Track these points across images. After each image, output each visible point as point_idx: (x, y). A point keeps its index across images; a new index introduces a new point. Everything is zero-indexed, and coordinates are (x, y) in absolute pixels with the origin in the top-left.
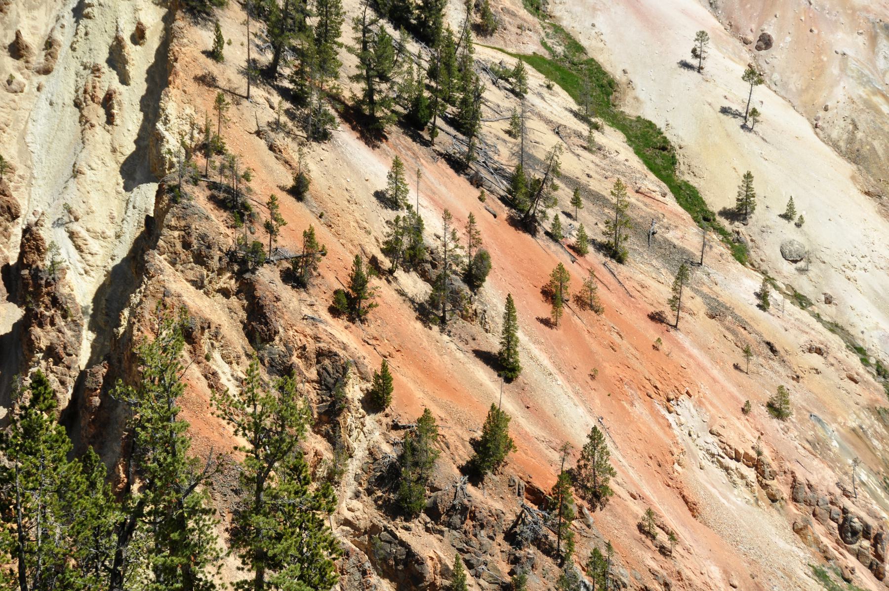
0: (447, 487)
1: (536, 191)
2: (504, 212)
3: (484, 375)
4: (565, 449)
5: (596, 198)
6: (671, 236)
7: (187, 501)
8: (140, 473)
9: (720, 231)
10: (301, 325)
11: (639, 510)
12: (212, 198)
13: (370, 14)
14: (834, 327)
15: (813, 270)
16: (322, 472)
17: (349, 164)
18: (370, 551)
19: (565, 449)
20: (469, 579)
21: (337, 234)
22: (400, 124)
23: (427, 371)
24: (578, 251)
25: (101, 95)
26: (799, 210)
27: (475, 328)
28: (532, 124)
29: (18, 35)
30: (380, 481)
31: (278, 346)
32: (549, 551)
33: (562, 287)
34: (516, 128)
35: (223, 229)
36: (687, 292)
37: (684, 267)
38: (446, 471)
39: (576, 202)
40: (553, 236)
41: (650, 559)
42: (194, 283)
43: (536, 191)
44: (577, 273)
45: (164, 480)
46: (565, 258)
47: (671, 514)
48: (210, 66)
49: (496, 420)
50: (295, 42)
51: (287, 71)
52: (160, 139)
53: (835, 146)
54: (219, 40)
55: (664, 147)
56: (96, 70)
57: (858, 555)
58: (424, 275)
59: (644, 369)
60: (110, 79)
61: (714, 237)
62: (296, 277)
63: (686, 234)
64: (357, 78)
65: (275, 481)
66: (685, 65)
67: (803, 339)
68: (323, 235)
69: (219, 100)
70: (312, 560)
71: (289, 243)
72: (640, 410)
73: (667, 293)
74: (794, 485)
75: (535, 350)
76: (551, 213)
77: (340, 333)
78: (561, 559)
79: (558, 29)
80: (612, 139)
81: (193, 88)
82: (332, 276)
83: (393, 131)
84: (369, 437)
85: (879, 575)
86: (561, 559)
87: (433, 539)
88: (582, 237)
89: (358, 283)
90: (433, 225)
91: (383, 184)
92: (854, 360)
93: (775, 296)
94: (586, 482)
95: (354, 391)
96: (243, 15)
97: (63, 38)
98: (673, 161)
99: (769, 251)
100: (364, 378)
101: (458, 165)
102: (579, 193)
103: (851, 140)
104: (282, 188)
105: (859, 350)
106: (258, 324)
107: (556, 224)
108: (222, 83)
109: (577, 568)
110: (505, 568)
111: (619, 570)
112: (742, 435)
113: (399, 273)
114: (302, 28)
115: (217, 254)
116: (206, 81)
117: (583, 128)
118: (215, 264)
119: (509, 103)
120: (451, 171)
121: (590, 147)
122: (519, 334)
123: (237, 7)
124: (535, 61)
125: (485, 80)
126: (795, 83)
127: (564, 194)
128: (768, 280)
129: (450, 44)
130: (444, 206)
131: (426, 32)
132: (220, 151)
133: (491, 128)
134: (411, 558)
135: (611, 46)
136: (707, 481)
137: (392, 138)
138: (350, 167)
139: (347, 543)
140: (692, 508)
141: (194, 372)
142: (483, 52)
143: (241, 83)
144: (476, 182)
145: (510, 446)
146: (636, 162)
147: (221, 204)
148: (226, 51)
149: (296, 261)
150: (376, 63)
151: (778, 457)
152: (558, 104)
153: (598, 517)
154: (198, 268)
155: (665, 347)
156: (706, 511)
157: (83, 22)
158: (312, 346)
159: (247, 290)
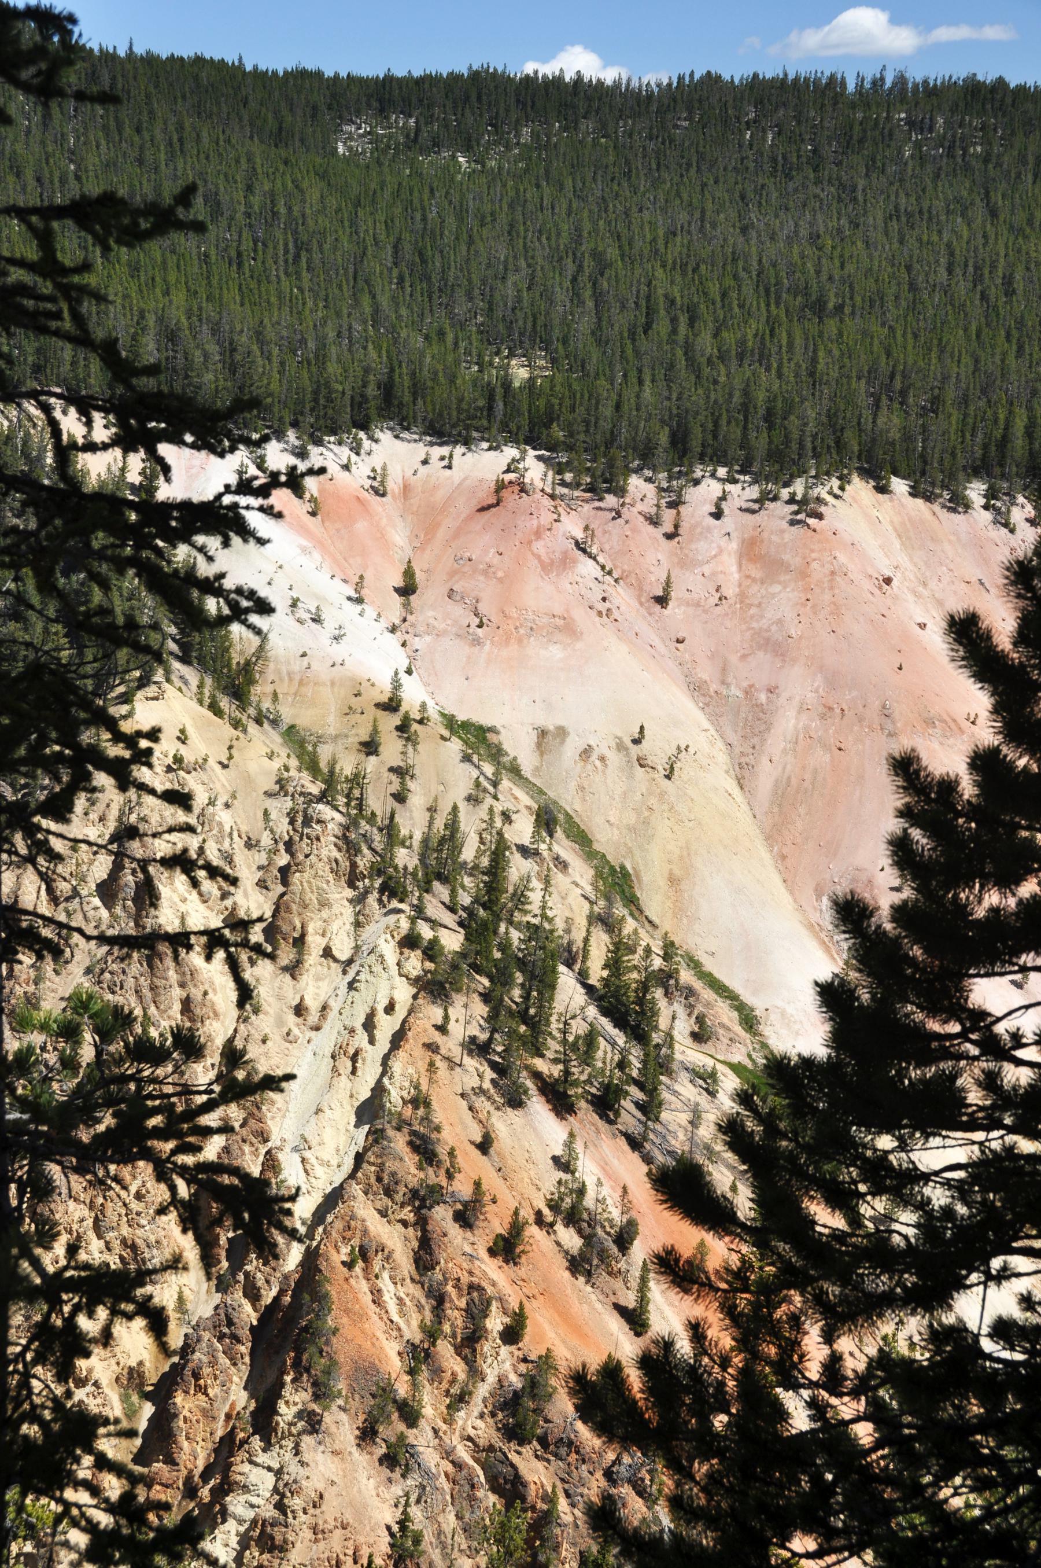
17: (535, 1129)
21: (511, 1187)
22: (591, 1103)
25: (351, 1051)
29: (302, 998)
35: (413, 1170)
42: (380, 1212)
56: (352, 1031)
60: (361, 1039)
97: (335, 1005)
104: (472, 1143)
115: (402, 1190)
120: (626, 1148)
137: (580, 1114)
154: (385, 1199)
157: (353, 993)
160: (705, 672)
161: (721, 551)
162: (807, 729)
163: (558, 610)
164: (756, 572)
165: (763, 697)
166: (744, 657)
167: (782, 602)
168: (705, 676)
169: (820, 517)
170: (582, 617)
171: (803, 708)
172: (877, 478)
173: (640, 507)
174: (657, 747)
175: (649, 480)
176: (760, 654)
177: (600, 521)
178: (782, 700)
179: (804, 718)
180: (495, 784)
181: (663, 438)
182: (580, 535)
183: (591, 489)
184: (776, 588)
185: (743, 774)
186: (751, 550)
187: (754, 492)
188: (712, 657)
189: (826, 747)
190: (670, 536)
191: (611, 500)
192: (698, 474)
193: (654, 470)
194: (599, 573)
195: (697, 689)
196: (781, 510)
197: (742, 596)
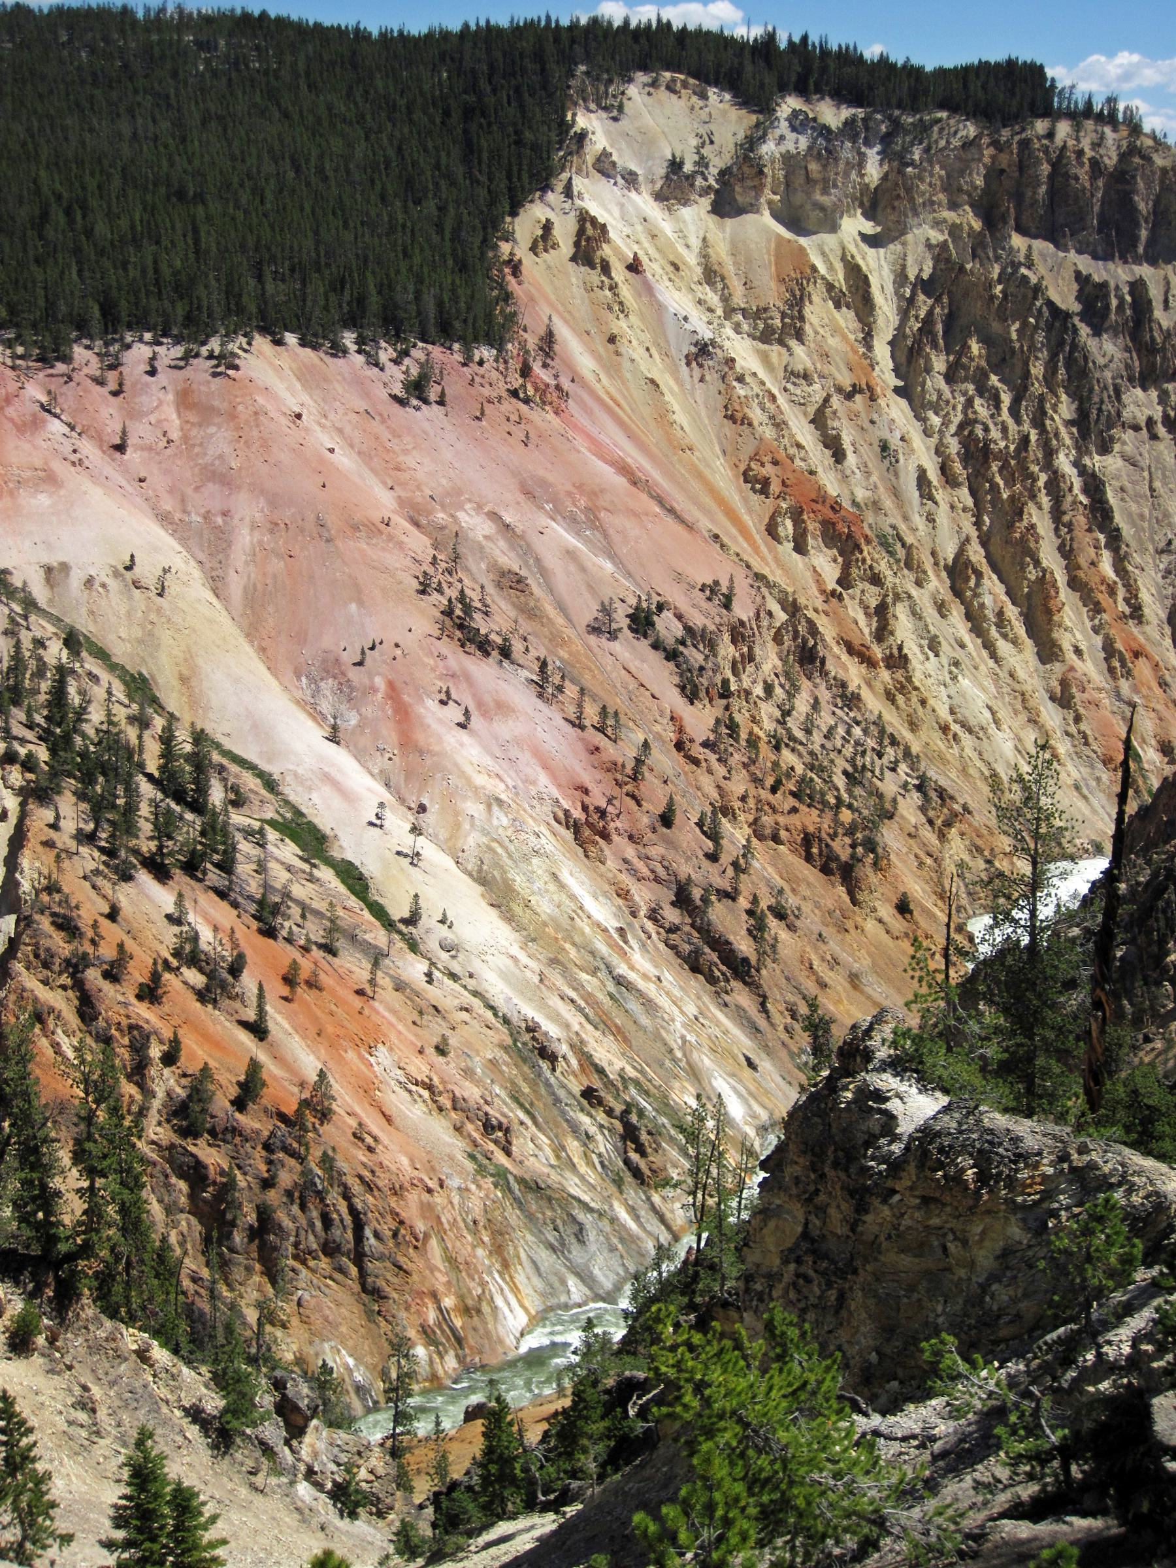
0: (222, 1115)
1: (276, 910)
2: (255, 925)
3: (244, 1037)
4: (302, 1085)
5: (317, 913)
6: (367, 937)
7: (40, 1134)
8: (10, 1115)
9: (400, 932)
10: (117, 1008)
11: (353, 1123)
12: (53, 923)
13: (160, 796)
14: (476, 994)
15: (461, 957)
16: (135, 1108)
18: (170, 1161)
19: (302, 1085)
20: (239, 1177)
23: (206, 1037)
24: (306, 949)
26: (450, 917)
27: (237, 1005)
28: (272, 865)
30: (175, 1114)
31: (101, 1023)
32: (293, 1154)
33: (296, 975)
34: (261, 868)
36: (379, 974)
37: (377, 958)
38: (221, 1104)
39: (303, 916)
40: (289, 940)
41: (361, 1156)
43: (276, 910)
44: (306, 965)
45: (24, 1120)
46: (296, 954)
47: (374, 1124)
48: (52, 834)
49: (254, 1067)
50: (110, 816)
51: (104, 835)
52: (17, 884)
53: (470, 875)
54: (58, 817)
55: (361, 877)
57: (496, 1142)
58: (201, 971)
59: (353, 1027)
61: (396, 937)
62: (112, 975)
63: (378, 936)
64: (151, 838)
65: (102, 1116)
66: (371, 824)
67: (456, 1002)
68: (130, 945)
69: (58, 856)
70: (129, 1170)
71: (107, 952)
72: (351, 1055)
73: (366, 976)
74: (454, 1100)
75: (279, 1018)
76: (287, 924)
77: (143, 1012)
78: (301, 1159)
79: (287, 802)
80: (326, 874)
81: (40, 849)
82: (138, 974)
83: (177, 873)
84: (166, 1083)
85: (508, 1153)
86: (301, 1159)
87: (213, 1151)
88: (308, 940)
89: (156, 977)
90: (206, 936)
91: (170, 908)
92: (489, 1014)
93: (437, 974)
94: (316, 1105)
95: (155, 1051)
96: (74, 799)
98: (367, 887)
99: (431, 945)
100: (161, 1042)
101: (222, 894)
102: (306, 910)
103: (480, 871)
105: (492, 1008)
106: (87, 1008)
107: (291, 932)
108: (59, 845)
109: (313, 1165)
110: (263, 1167)
111: (341, 1164)
112: (419, 1068)
113: (184, 970)
114: (114, 806)
116: (49, 844)
117: (306, 867)
118: (56, 968)
119: (255, 851)
121: (312, 879)
122: (268, 1008)
123: (68, 794)
124: (272, 823)
125: (239, 837)
126: (443, 834)
127: (295, 911)
128: (432, 964)
129: (215, 814)
130: (212, 923)
131: (198, 807)
132: (59, 891)
133: (244, 869)
134: (199, 1165)
135: (323, 811)
136: (398, 1100)
138: (151, 897)
139: (154, 1156)
140: (388, 1119)
141: (44, 1042)
142: (237, 818)
143: (72, 845)
144: (235, 905)
145: (264, 1084)
146: (342, 889)
147: (59, 927)
148: (62, 823)
149: (111, 964)
150: (164, 827)
151: (443, 1082)
152: (289, 851)
153: (326, 1129)
155: (366, 1012)
156: (397, 1121)
158: (125, 1022)
159: (79, 985)
160: (168, 504)
161: (161, 403)
162: (260, 542)
163: (38, 463)
164: (193, 417)
165: (219, 520)
166: (197, 489)
167: (219, 441)
168: (168, 508)
169: (236, 368)
170: (57, 466)
171: (254, 527)
172: (272, 334)
173: (86, 370)
174: (147, 571)
175: (87, 347)
176: (210, 485)
177: (54, 384)
178: (236, 521)
179: (257, 534)
180: (26, 618)
181: (96, 312)
182: (44, 399)
183: (41, 359)
184: (212, 430)
185: (217, 585)
186: (185, 399)
187: (179, 351)
188: (171, 491)
189: (279, 556)
190: (115, 394)
191: (61, 367)
192: (129, 339)
193: (92, 338)
194: (66, 430)
195: (164, 518)
196: (202, 366)
197: (185, 438)
